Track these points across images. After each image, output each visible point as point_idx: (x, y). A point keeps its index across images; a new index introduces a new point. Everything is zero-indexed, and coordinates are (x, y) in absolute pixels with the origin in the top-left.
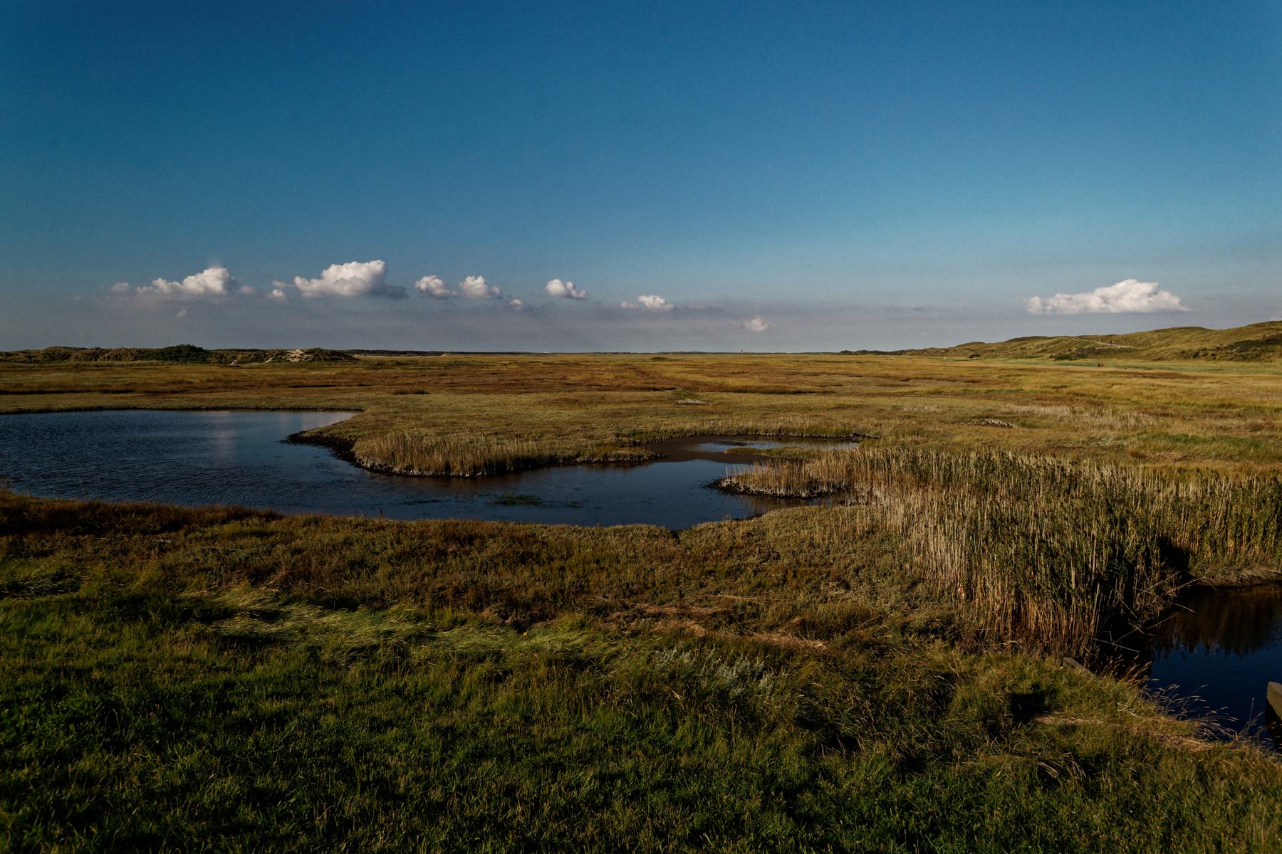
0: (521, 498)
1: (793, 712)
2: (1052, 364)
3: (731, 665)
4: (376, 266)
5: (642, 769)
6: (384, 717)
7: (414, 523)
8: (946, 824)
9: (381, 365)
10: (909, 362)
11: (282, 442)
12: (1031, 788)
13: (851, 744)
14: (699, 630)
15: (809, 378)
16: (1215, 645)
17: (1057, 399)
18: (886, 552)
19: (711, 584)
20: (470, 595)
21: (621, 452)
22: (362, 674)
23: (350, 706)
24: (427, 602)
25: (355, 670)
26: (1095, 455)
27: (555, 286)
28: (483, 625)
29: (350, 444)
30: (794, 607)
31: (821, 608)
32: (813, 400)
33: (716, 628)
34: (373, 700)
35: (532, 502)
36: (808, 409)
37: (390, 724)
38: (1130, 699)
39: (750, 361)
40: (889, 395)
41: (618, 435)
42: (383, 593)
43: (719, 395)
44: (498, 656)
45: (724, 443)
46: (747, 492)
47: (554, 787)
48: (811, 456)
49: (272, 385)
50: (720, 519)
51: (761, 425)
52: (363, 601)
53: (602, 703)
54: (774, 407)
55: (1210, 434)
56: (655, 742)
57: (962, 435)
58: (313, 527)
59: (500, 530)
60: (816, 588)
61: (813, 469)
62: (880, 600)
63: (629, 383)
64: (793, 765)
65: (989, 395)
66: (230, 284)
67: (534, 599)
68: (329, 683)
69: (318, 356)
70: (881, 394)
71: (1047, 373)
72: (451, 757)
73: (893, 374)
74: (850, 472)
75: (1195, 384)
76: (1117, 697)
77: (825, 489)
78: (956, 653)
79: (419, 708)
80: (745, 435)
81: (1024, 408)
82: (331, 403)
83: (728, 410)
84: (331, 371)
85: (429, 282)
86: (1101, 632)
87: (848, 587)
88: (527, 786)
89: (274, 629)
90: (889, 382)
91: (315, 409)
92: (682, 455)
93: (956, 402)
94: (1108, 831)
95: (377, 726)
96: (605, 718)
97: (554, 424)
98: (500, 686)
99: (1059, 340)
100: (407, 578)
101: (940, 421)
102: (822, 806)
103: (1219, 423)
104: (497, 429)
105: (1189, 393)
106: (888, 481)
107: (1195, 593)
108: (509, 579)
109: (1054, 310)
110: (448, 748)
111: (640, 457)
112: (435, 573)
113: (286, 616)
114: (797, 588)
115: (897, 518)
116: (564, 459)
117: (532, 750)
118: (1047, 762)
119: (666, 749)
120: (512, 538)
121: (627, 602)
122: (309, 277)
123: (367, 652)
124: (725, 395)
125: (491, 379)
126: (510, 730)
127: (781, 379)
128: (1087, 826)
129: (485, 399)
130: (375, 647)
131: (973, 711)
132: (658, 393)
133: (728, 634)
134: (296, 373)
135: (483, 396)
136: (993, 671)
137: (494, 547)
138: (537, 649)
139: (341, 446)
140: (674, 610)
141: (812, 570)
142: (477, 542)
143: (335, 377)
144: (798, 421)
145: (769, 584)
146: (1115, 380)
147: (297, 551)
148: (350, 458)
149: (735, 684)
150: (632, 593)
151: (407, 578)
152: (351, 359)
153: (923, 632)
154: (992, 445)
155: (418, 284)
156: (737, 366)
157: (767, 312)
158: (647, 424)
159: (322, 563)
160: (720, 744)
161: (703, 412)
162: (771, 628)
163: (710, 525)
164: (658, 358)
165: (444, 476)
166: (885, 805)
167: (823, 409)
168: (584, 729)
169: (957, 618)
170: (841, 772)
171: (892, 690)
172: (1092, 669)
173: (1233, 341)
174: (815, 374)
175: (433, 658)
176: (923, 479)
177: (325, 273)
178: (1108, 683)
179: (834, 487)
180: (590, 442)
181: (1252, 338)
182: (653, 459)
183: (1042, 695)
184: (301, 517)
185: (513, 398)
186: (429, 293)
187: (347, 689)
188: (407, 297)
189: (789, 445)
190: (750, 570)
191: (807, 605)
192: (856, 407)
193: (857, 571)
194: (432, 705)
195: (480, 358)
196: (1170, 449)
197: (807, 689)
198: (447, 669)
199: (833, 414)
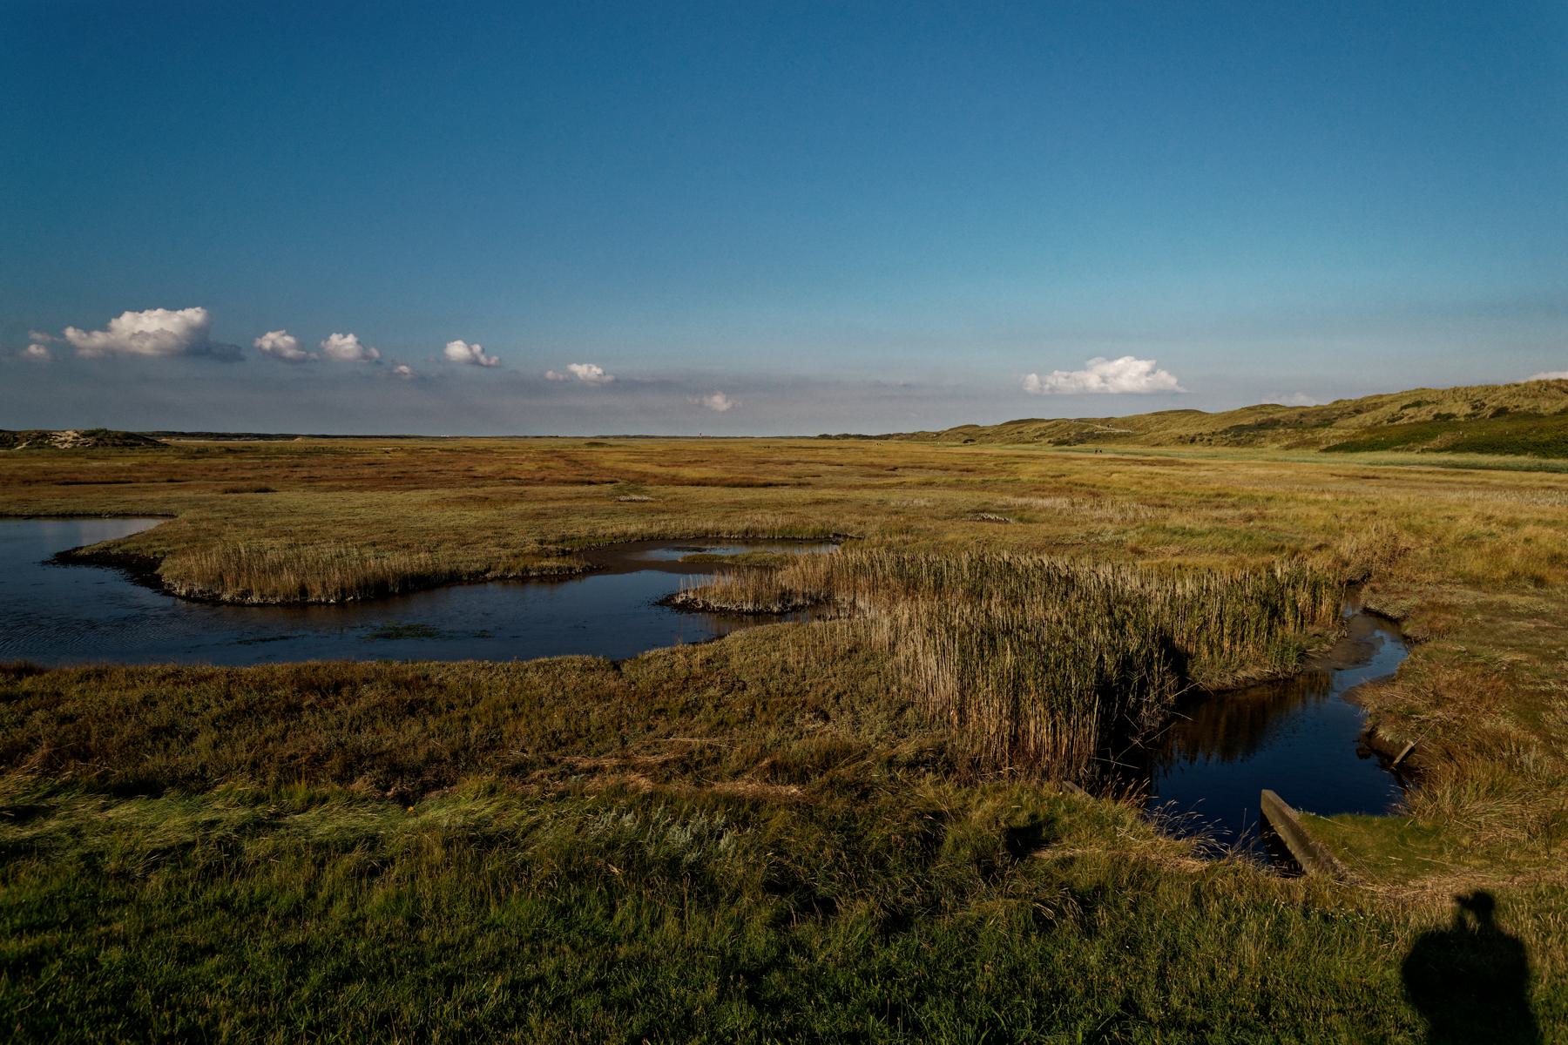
0: (409, 628)
1: (759, 876)
2: (1051, 450)
3: (685, 825)
4: (195, 315)
5: (568, 970)
6: (200, 942)
7: (252, 669)
8: (933, 989)
9: (202, 452)
10: (897, 448)
11: (44, 563)
12: (1026, 934)
13: (828, 907)
14: (645, 784)
15: (783, 468)
16: (1215, 757)
17: (1055, 490)
18: (871, 673)
19: (662, 725)
20: (335, 764)
21: (545, 563)
22: (168, 885)
23: (149, 931)
24: (272, 777)
25: (156, 881)
26: (1095, 552)
27: (457, 349)
28: (352, 801)
29: (155, 563)
30: (763, 746)
31: (795, 746)
32: (786, 494)
33: (668, 779)
34: (185, 919)
35: (425, 633)
36: (779, 505)
37: (210, 950)
38: (1129, 822)
39: (710, 447)
40: (874, 487)
41: (541, 542)
42: (203, 768)
43: (671, 489)
44: (373, 841)
45: (678, 549)
46: (706, 608)
47: (447, 1007)
48: (784, 562)
49: (27, 482)
50: (672, 645)
51: (724, 526)
52: (173, 782)
53: (516, 889)
54: (740, 503)
55: (1207, 526)
56: (587, 932)
57: (955, 533)
58: (93, 683)
59: (379, 674)
60: (790, 722)
61: (786, 578)
62: (865, 730)
63: (557, 476)
64: (759, 939)
65: (984, 486)
67: (426, 762)
68: (117, 902)
69: (101, 440)
70: (865, 486)
71: (1043, 461)
72: (300, 985)
73: (877, 463)
74: (828, 582)
75: (1192, 472)
76: (1117, 821)
77: (800, 601)
78: (948, 786)
79: (257, 922)
80: (704, 538)
81: (1021, 501)
82: (122, 507)
83: (684, 508)
84: (125, 461)
85: (273, 339)
86: (1101, 750)
87: (827, 718)
88: (410, 1010)
89: (27, 833)
90: (873, 471)
91: (98, 516)
92: (631, 564)
93: (950, 494)
94: (1103, 972)
95: (189, 955)
96: (522, 908)
97: (455, 529)
98: (376, 881)
99: (1057, 423)
100: (241, 745)
101: (932, 517)
102: (792, 986)
103: (1216, 513)
104: (376, 538)
105: (1186, 482)
106: (873, 588)
107: (1194, 699)
108: (390, 738)
109: (1052, 389)
110: (297, 973)
111: (570, 569)
112: (283, 737)
113: (48, 813)
114: (767, 723)
115: (882, 635)
116: (470, 575)
117: (420, 962)
118: (1043, 903)
119: (600, 940)
120: (397, 684)
121: (553, 755)
122: (88, 329)
123: (177, 853)
124: (679, 489)
125: (367, 471)
126: (389, 939)
127: (751, 469)
128: (1083, 970)
129: (358, 498)
130: (189, 846)
131: (966, 852)
132: (593, 488)
133: (681, 786)
134: (67, 464)
135: (355, 494)
136: (989, 804)
137: (370, 695)
138: (430, 827)
139: (139, 567)
140: (615, 762)
141: (786, 700)
142: (345, 691)
143: (130, 470)
144: (768, 520)
145: (733, 721)
146: (1114, 468)
147: (65, 719)
148: (156, 584)
149: (689, 847)
150: (560, 744)
151: (241, 745)
152: (156, 445)
153: (912, 765)
154: (988, 543)
155: (258, 342)
156: (695, 453)
157: (734, 387)
158: (580, 527)
159: (110, 733)
160: (670, 924)
161: (652, 511)
162: (736, 775)
163: (661, 651)
164: (594, 444)
165: (299, 603)
166: (865, 976)
167: (798, 505)
168: (493, 926)
169: (949, 746)
170: (816, 943)
171: (876, 836)
172: (1091, 792)
173: (1226, 425)
174: (789, 463)
175: (277, 853)
176: (912, 588)
177: (114, 323)
178: (1107, 806)
179: (811, 598)
180: (503, 552)
181: (1245, 422)
182: (588, 571)
183: (1040, 826)
184: (74, 669)
185: (397, 497)
186: (275, 354)
187: (144, 908)
188: (242, 359)
189: (759, 549)
190: (709, 705)
191: (778, 744)
192: (836, 502)
193: (837, 698)
194: (275, 917)
195: (350, 443)
196: (1168, 544)
197: (778, 847)
198: (298, 866)
199: (810, 511)
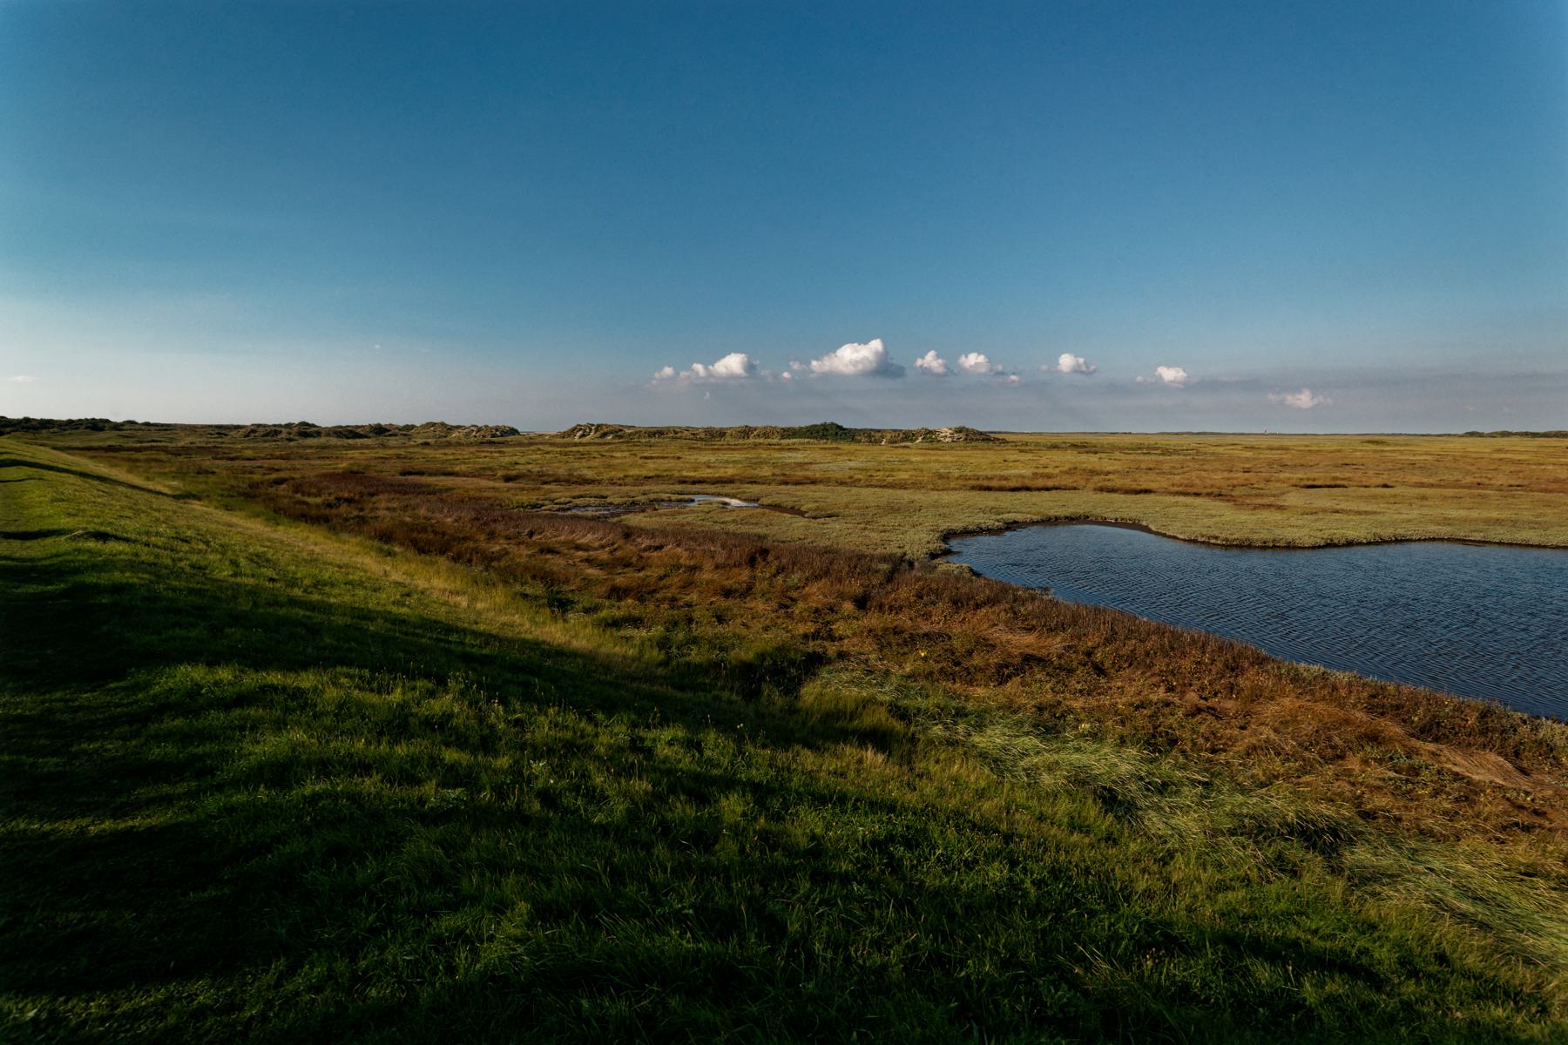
4: (876, 345)
27: (1066, 361)
66: (750, 367)
85: (931, 360)
186: (926, 371)
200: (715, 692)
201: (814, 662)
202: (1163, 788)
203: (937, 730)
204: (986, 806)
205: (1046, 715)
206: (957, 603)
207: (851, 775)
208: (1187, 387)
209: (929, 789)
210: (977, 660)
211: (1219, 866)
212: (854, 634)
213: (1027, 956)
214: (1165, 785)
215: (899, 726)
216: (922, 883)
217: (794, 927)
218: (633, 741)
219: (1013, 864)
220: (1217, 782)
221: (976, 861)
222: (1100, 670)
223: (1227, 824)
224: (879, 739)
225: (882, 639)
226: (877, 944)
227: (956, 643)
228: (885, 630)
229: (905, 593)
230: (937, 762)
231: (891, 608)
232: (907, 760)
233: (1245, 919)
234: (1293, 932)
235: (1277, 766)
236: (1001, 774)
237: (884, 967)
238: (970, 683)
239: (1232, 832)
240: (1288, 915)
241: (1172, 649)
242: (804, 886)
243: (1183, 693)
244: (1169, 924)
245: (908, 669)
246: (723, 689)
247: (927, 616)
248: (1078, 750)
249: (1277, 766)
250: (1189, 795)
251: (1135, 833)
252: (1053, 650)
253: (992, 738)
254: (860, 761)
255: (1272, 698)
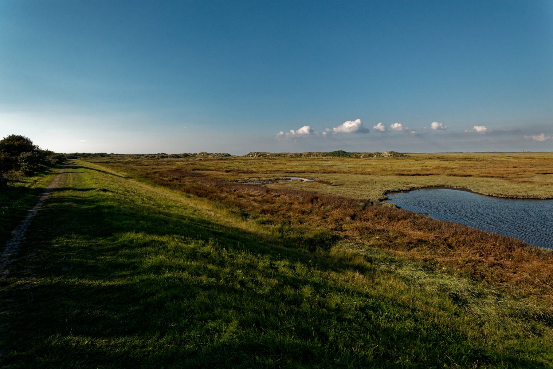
4: (358, 121)
27: (434, 125)
66: (311, 131)
186: (378, 131)
200: (299, 249)
201: (335, 239)
202: (479, 295)
203: (383, 267)
204: (404, 297)
205: (428, 263)
206: (390, 218)
207: (350, 282)
208: (487, 134)
209: (381, 289)
210: (399, 241)
211: (506, 329)
212: (351, 229)
213: (424, 358)
214: (480, 294)
215: (368, 265)
216: (380, 325)
217: (331, 338)
218: (271, 264)
219: (416, 321)
220: (503, 294)
221: (401, 319)
222: (450, 246)
223: (508, 312)
224: (361, 269)
225: (361, 231)
226: (363, 347)
227: (390, 234)
228: (362, 228)
229: (370, 214)
230: (384, 279)
231: (365, 220)
232: (372, 278)
233: (518, 352)
234: (540, 359)
235: (531, 289)
236: (410, 285)
237: (366, 356)
238: (396, 249)
239: (511, 316)
240: (538, 352)
241: (482, 239)
242: (335, 323)
243: (487, 257)
244: (484, 351)
245: (371, 243)
246: (302, 247)
247: (379, 223)
248: (442, 278)
249: (531, 289)
250: (491, 299)
251: (467, 313)
252: (430, 238)
253: (406, 271)
254: (354, 277)
255: (528, 261)
